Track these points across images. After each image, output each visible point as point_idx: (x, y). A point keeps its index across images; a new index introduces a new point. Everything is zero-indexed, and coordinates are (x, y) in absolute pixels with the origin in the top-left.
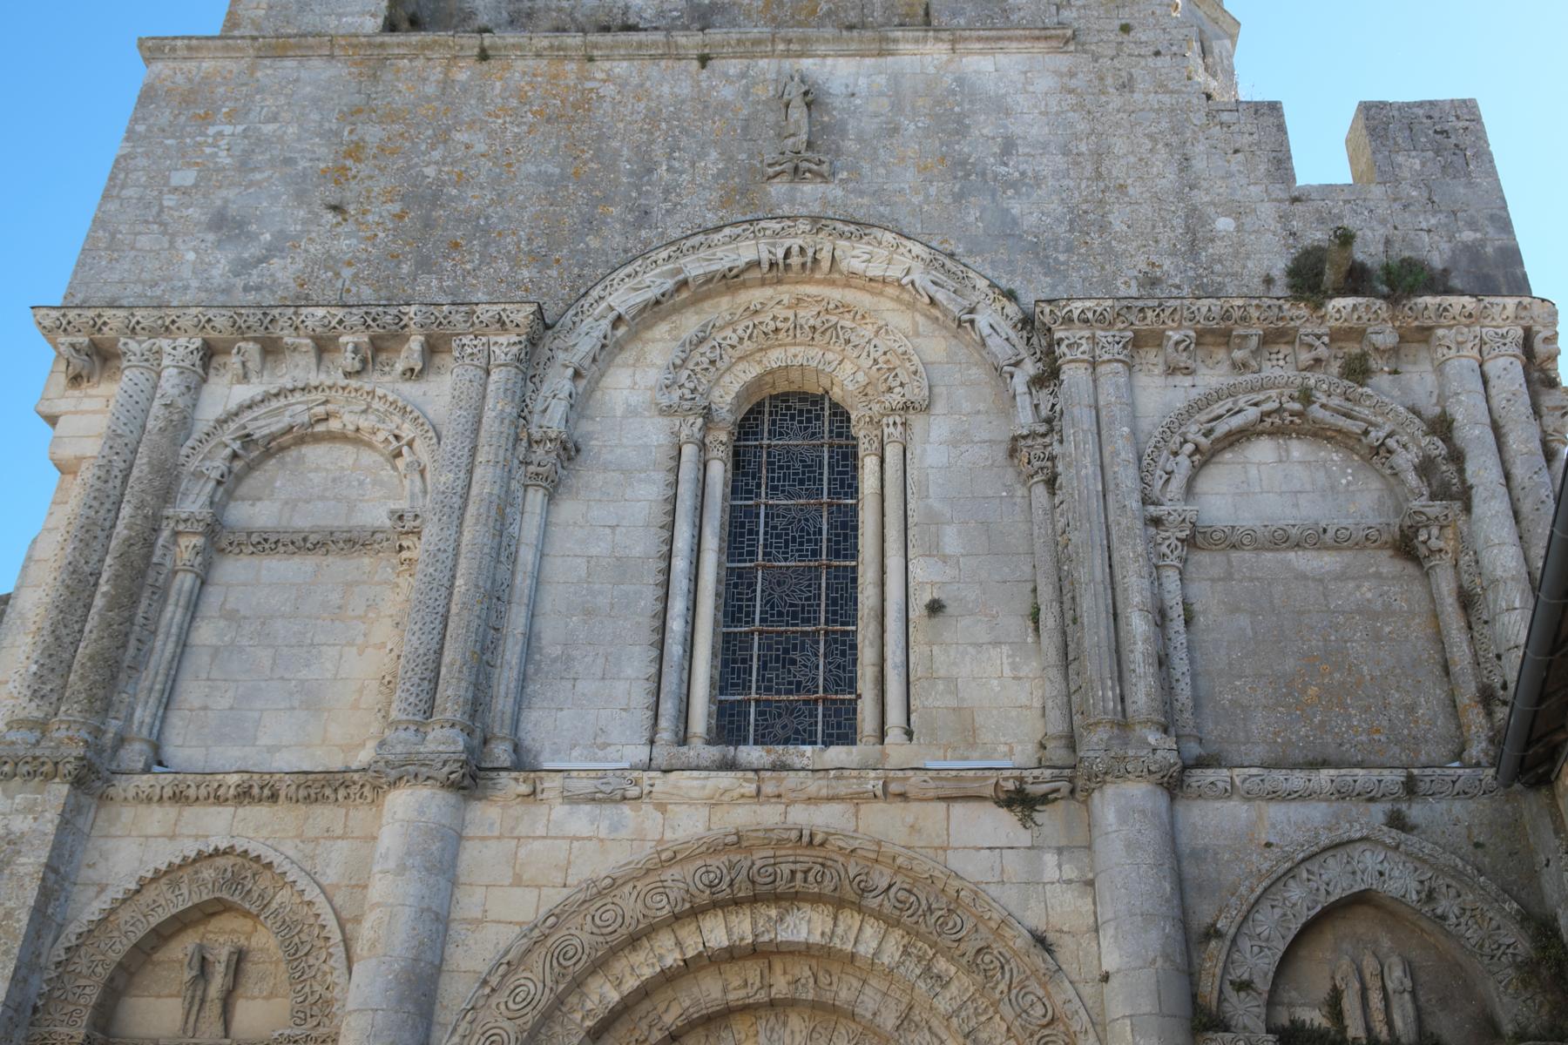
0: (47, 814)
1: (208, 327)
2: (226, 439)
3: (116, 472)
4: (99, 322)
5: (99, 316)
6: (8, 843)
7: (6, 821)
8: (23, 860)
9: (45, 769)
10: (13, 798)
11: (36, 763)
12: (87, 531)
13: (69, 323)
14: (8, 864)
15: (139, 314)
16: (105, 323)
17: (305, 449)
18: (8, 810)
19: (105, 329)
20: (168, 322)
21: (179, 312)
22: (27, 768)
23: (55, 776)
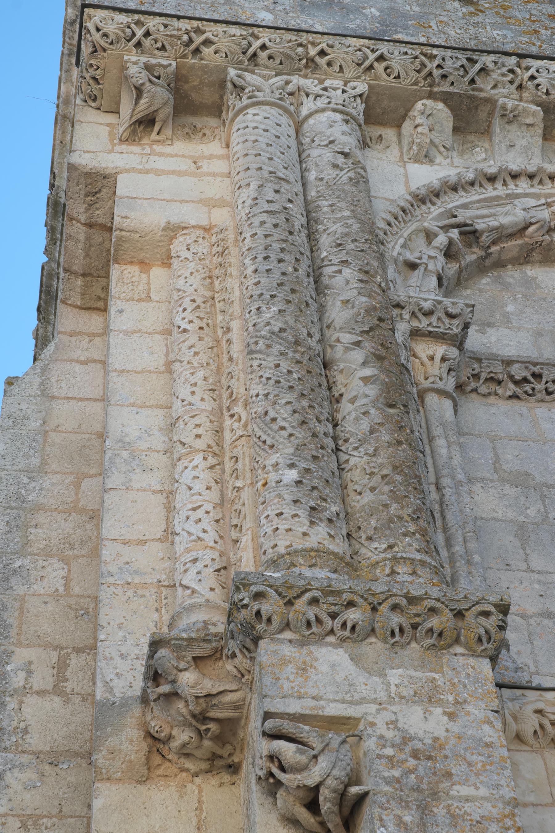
0: (469, 708)
1: (380, 67)
2: (430, 224)
3: (297, 225)
4: (198, 40)
5: (198, 31)
6: (415, 754)
7: (388, 716)
8: (465, 791)
9: (434, 622)
10: (382, 674)
11: (415, 609)
12: (293, 291)
13: (147, 34)
14: (435, 795)
15: (265, 37)
16: (207, 42)
17: (531, 271)
18: (382, 695)
19: (207, 51)
20: (313, 51)
21: (331, 40)
22: (396, 620)
23: (457, 641)
